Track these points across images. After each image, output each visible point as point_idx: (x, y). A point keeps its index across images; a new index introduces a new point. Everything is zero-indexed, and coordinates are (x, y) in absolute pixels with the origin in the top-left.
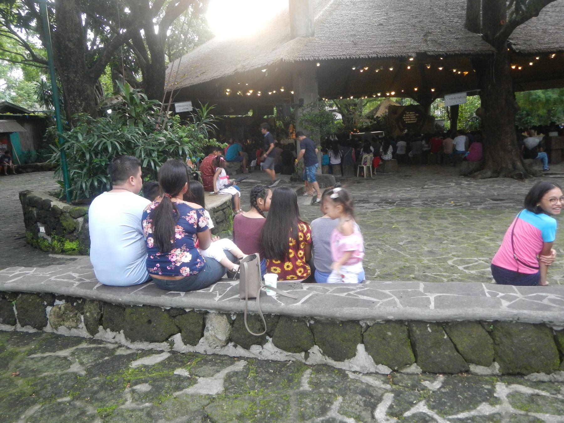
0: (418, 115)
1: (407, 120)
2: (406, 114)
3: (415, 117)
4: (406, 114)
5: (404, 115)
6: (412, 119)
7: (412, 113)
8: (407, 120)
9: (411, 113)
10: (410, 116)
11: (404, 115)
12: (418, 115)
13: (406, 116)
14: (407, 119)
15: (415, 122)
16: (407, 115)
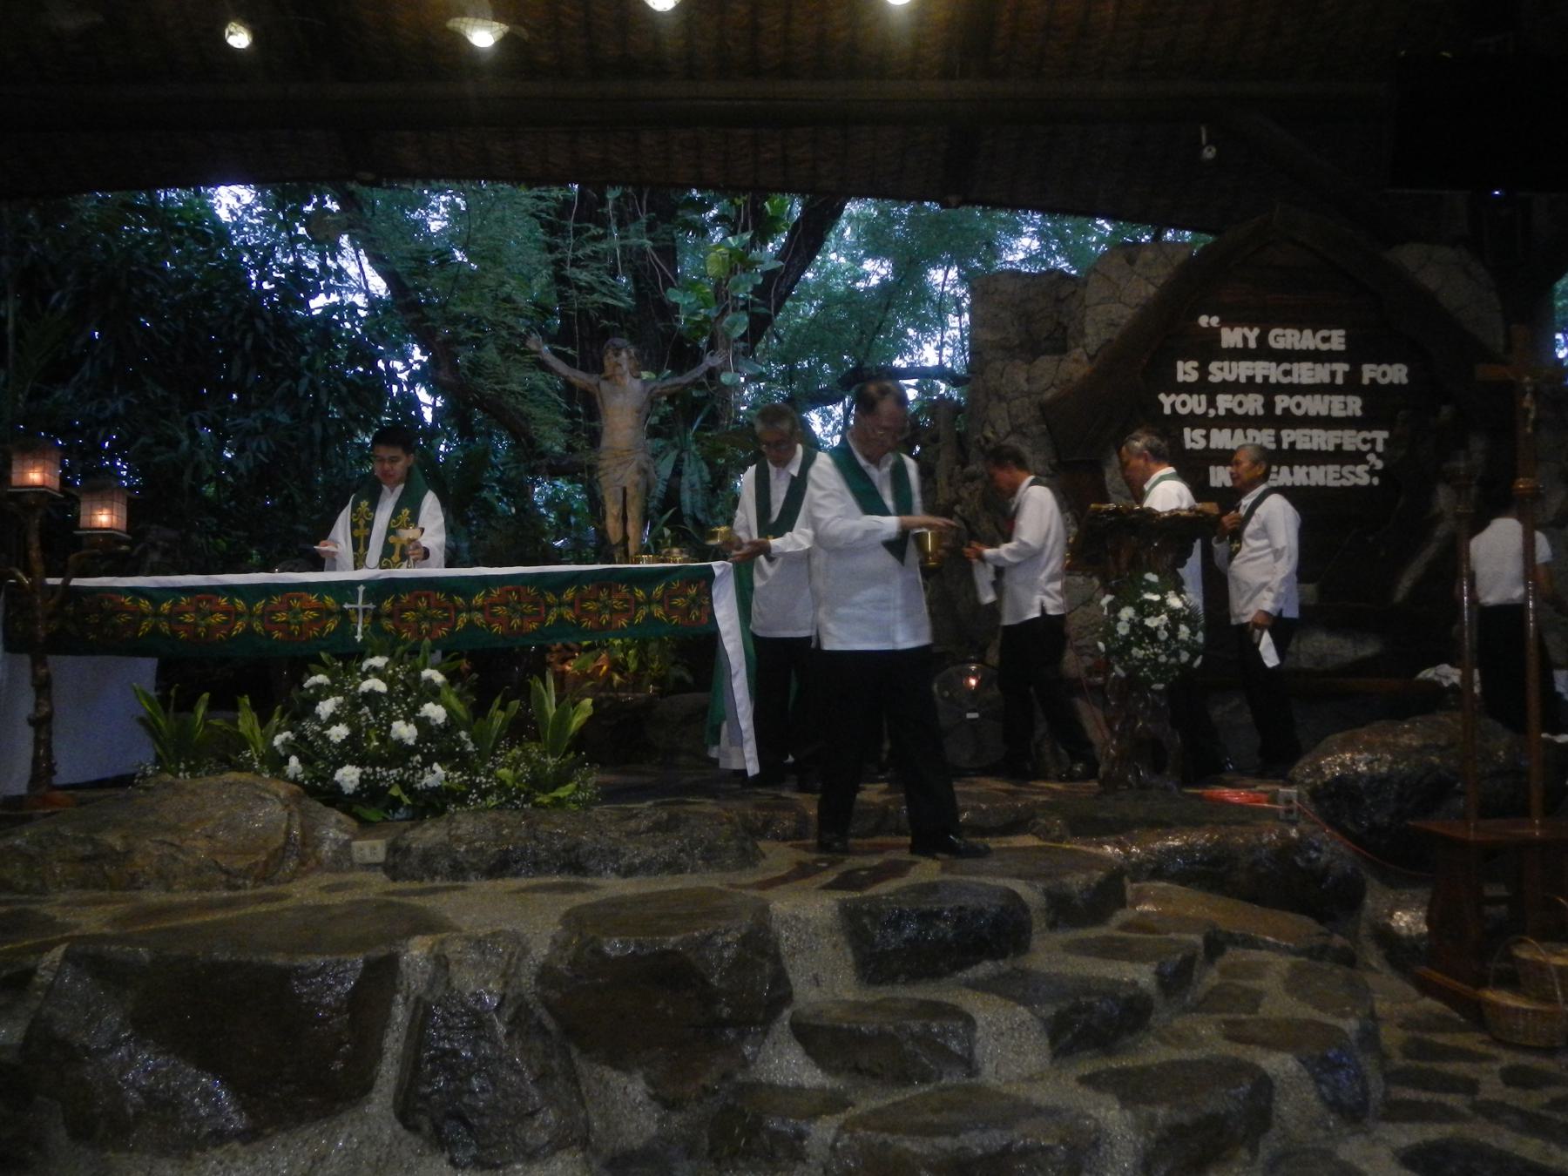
0: (1397, 374)
1: (1222, 439)
2: (1208, 349)
3: (1355, 405)
4: (1208, 349)
5: (1186, 371)
6: (1321, 440)
7: (1307, 340)
8: (1222, 439)
9: (1284, 338)
10: (1269, 390)
11: (1186, 371)
12: (1397, 374)
13: (1204, 387)
14: (1232, 421)
15: (1360, 476)
16: (1219, 372)
